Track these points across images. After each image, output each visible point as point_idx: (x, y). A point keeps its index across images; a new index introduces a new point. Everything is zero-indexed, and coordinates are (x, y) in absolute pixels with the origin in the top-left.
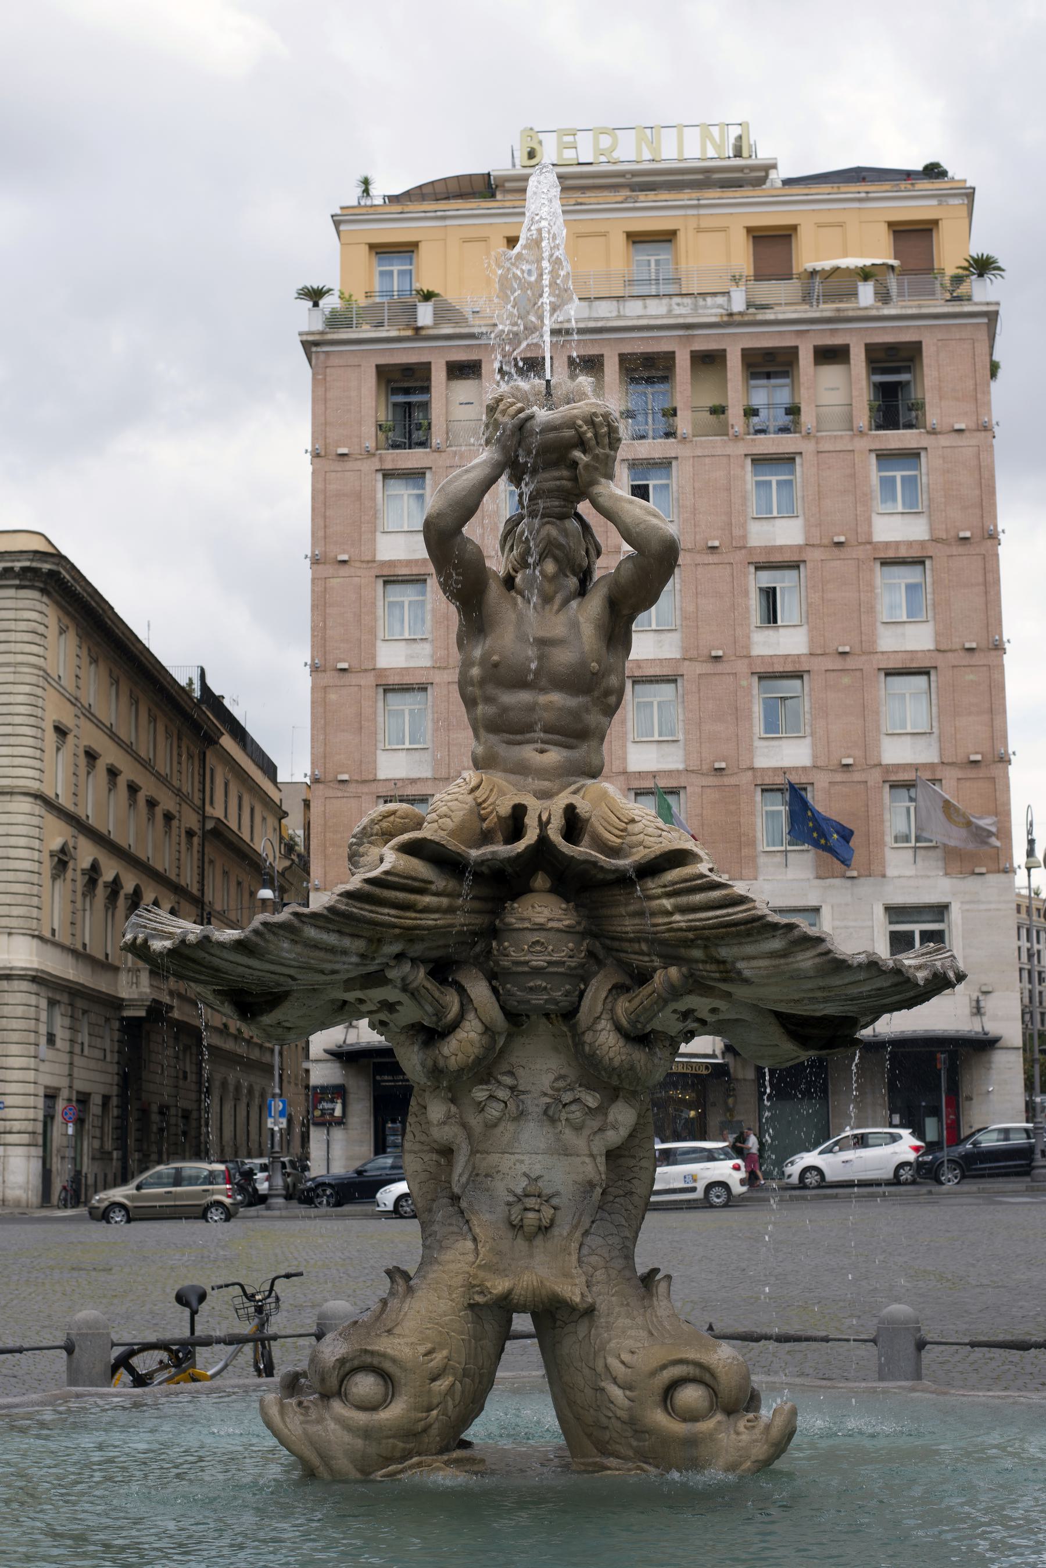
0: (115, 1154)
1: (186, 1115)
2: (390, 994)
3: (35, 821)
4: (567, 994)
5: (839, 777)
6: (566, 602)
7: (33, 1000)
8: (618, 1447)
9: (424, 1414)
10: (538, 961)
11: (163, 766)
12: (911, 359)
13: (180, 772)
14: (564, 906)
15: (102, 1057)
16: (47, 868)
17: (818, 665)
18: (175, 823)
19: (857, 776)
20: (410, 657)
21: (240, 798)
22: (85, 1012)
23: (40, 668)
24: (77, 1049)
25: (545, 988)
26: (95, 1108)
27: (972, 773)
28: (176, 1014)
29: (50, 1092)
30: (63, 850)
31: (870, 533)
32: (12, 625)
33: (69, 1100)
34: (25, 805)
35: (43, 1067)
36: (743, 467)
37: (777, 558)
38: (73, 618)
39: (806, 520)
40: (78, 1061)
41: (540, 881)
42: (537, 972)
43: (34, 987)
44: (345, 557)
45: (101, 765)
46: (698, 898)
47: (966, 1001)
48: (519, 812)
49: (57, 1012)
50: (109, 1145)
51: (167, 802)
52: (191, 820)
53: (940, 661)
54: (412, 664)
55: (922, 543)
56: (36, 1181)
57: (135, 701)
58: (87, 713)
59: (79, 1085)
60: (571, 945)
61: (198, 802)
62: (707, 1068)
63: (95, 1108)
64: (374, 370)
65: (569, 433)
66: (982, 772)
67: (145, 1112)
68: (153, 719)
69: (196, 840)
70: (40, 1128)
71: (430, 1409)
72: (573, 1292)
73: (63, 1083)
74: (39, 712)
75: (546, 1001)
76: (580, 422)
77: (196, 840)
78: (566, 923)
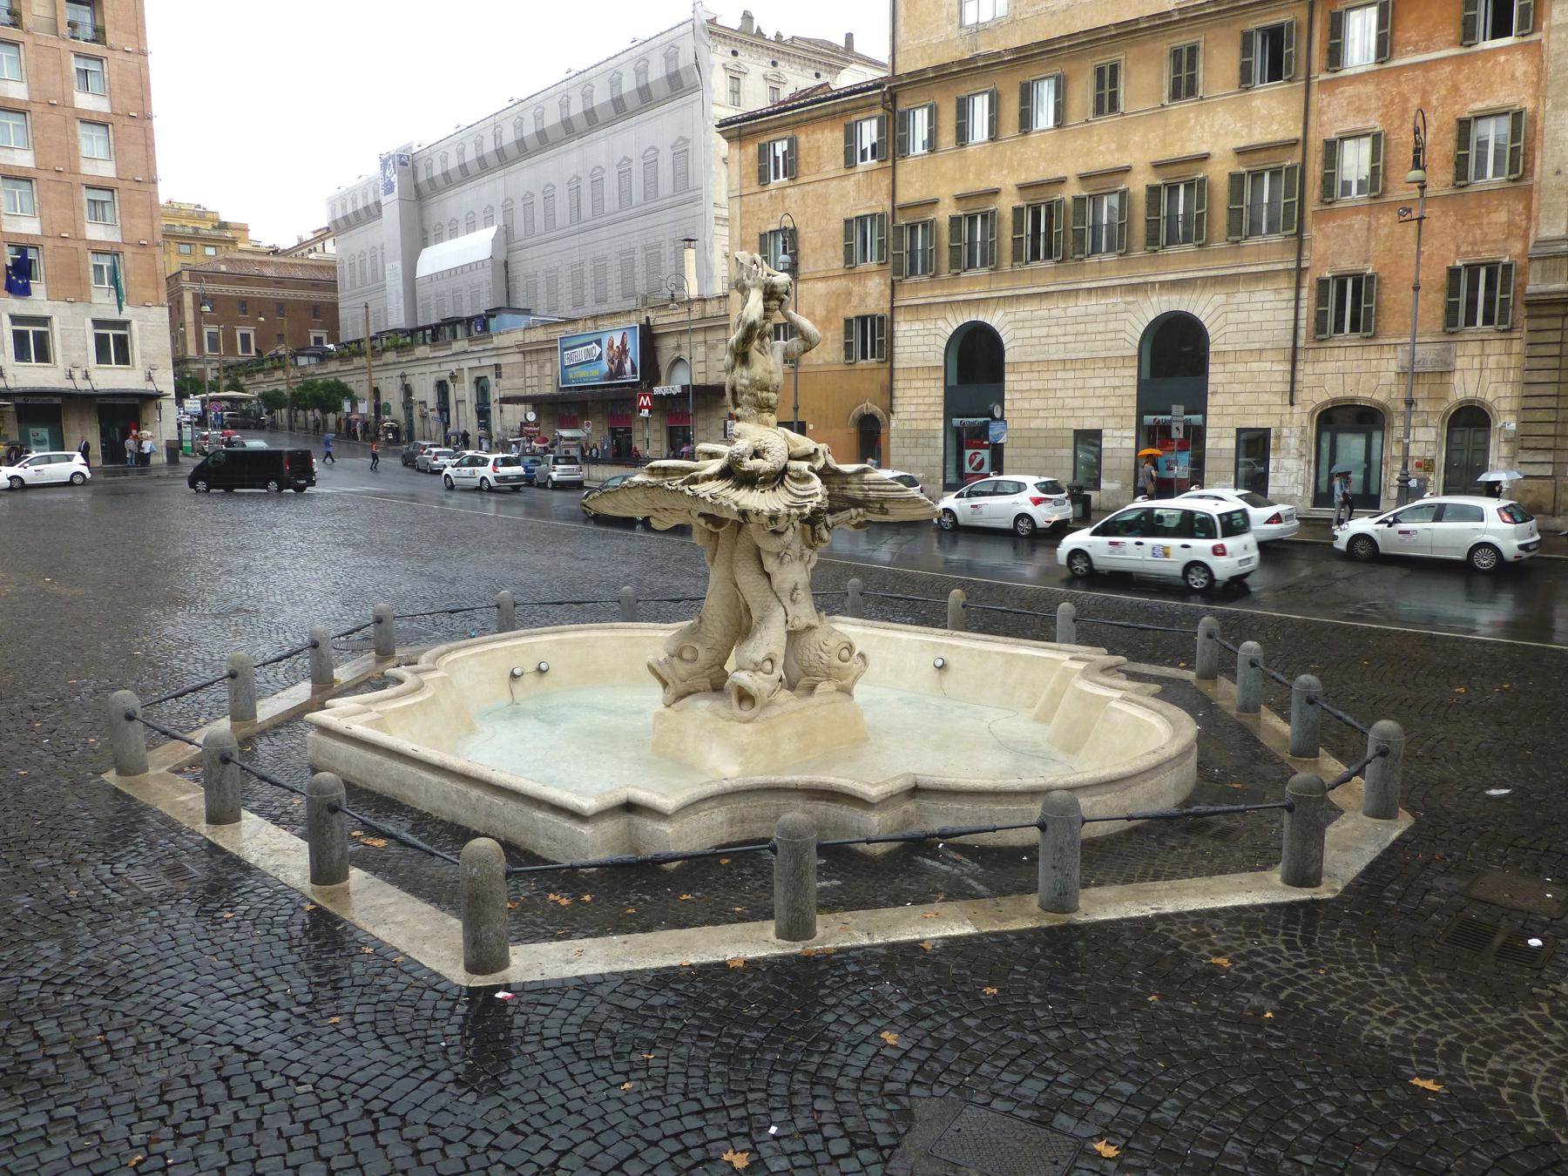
5: (59, 243)
17: (42, 175)
19: (71, 244)
27: (141, 250)
46: (883, 487)
53: (120, 184)
66: (148, 251)
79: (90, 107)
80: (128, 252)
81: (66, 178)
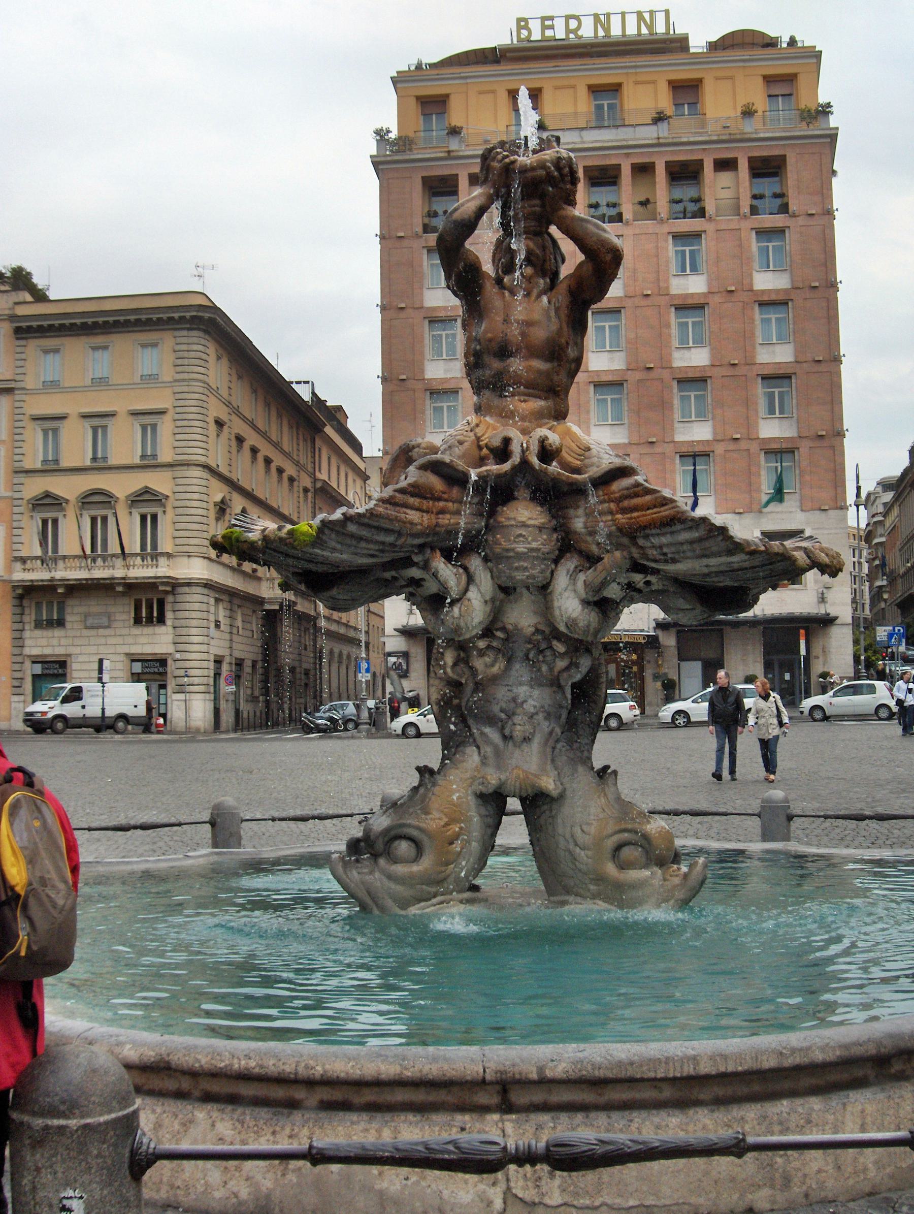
0: (261, 698)
1: (307, 673)
2: (415, 573)
3: (204, 482)
4: (542, 571)
5: (731, 446)
6: (539, 296)
7: (205, 599)
8: (582, 891)
9: (443, 869)
10: (521, 548)
11: (286, 446)
12: (779, 167)
13: (298, 450)
14: (539, 508)
15: (251, 635)
16: (212, 514)
17: (717, 372)
18: (296, 483)
20: (446, 371)
21: (338, 468)
22: (239, 606)
23: (205, 382)
24: (235, 631)
25: (526, 568)
26: (247, 669)
27: (817, 443)
28: (299, 608)
29: (218, 659)
30: (223, 501)
31: (752, 285)
32: (186, 354)
33: (230, 663)
34: (197, 472)
35: (212, 642)
36: (666, 241)
37: (690, 301)
38: (225, 349)
39: (709, 276)
40: (235, 638)
41: (523, 493)
42: (520, 556)
43: (206, 591)
44: (403, 305)
45: (246, 445)
47: (815, 593)
48: (507, 441)
49: (221, 607)
50: (257, 693)
51: (290, 470)
52: (307, 482)
54: (449, 376)
55: (786, 291)
56: (210, 716)
57: (267, 405)
58: (237, 412)
59: (237, 654)
60: (545, 537)
61: (310, 469)
62: (644, 639)
63: (247, 669)
64: (420, 179)
65: (542, 173)
66: (826, 443)
67: (279, 670)
68: (280, 416)
69: (310, 495)
70: (211, 682)
71: (447, 864)
72: (549, 784)
73: (225, 652)
74: (204, 411)
75: (528, 577)
76: (549, 164)
77: (310, 495)
78: (543, 520)
79: (769, 286)
80: (804, 448)
81: (738, 371)
